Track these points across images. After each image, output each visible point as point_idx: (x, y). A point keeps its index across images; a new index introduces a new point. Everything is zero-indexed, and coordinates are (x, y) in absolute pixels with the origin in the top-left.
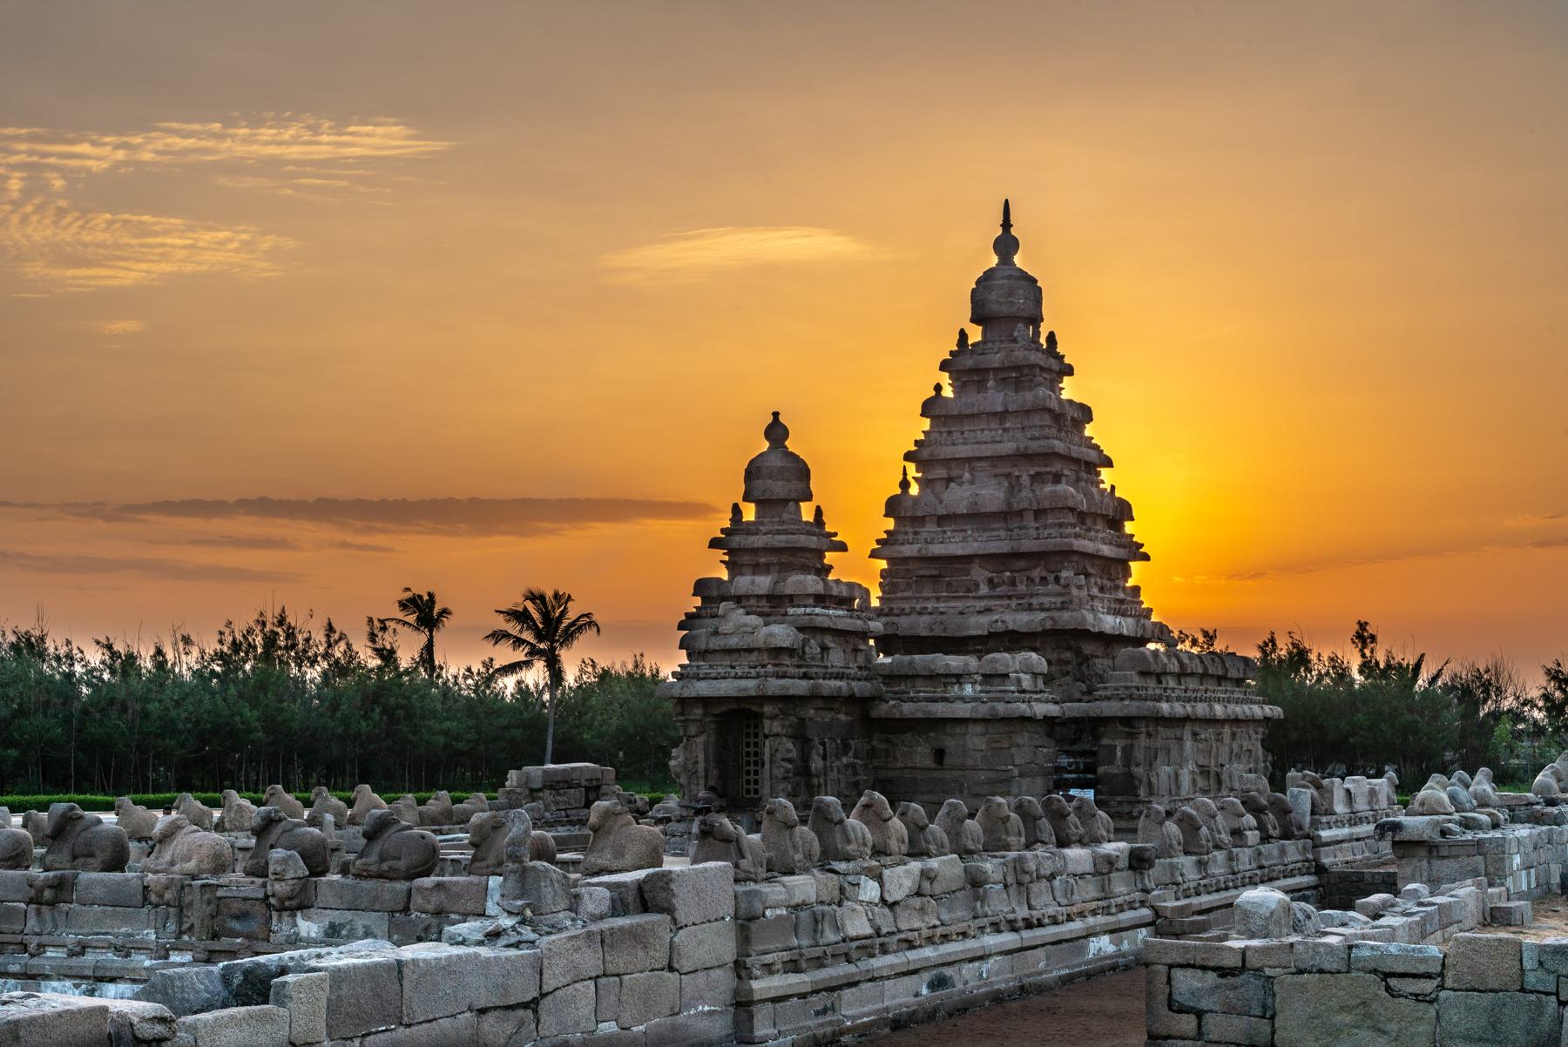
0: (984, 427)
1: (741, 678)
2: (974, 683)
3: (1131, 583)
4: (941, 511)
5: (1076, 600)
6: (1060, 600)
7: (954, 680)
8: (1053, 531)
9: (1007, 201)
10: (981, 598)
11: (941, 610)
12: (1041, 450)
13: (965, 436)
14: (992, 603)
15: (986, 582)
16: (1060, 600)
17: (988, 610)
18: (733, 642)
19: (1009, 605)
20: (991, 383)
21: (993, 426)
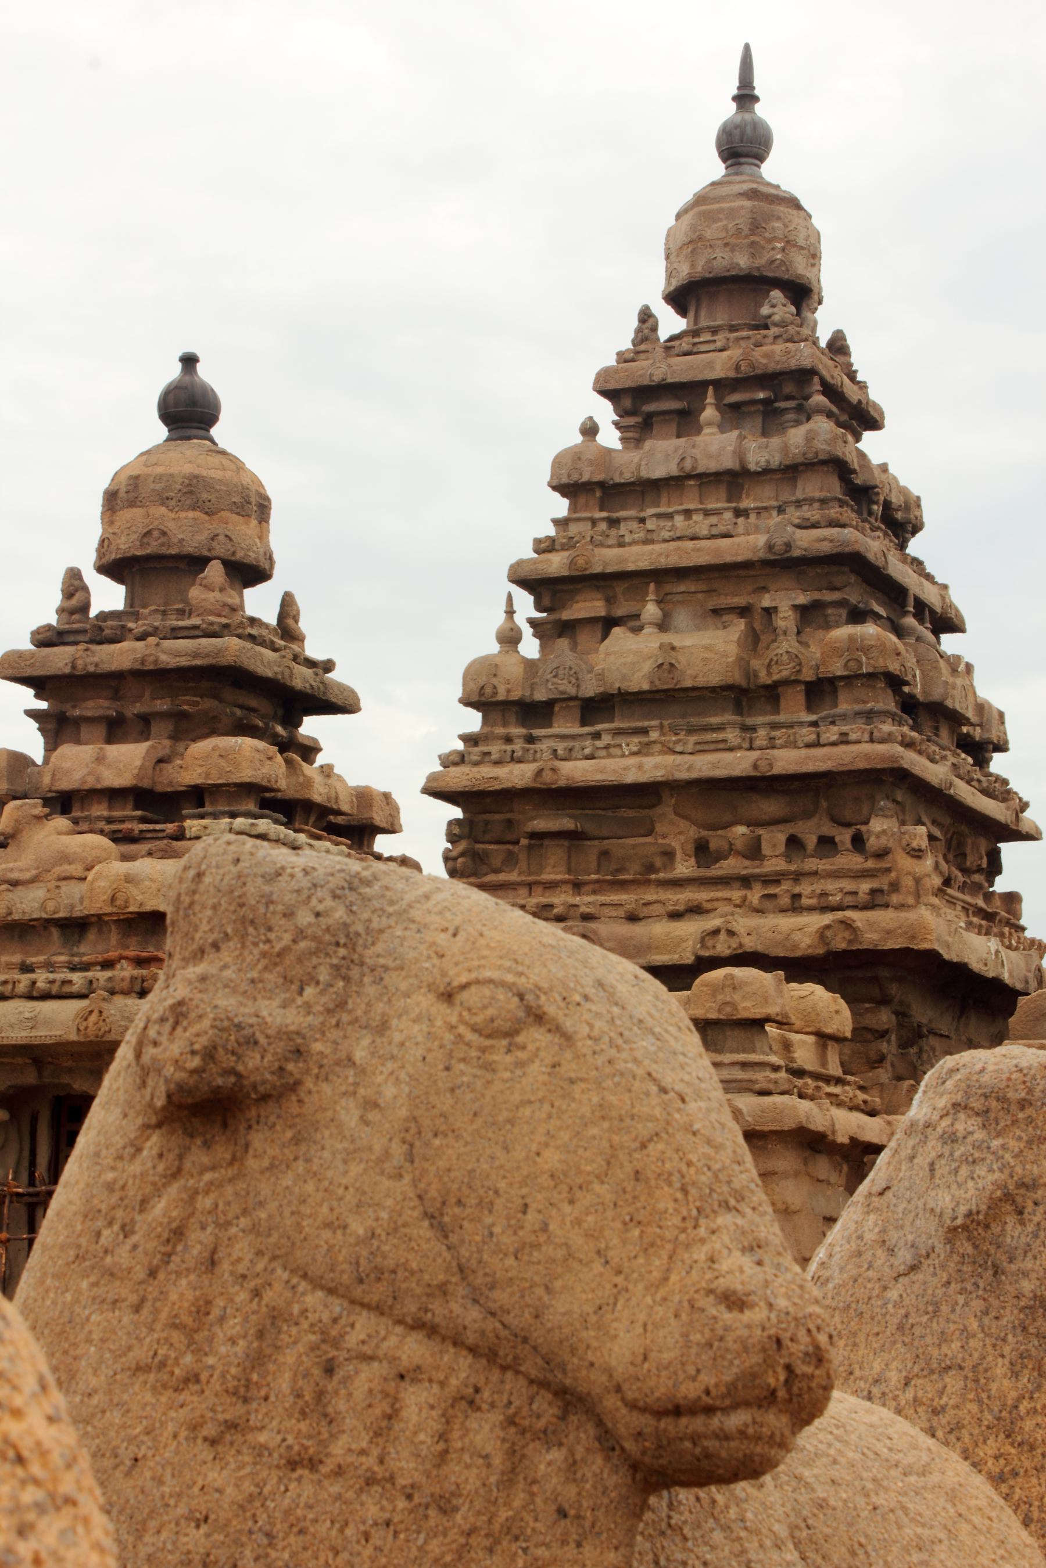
0: (691, 506)
1: (46, 996)
3: (1001, 885)
4: (590, 689)
5: (908, 882)
6: (865, 886)
9: (747, 48)
11: (584, 909)
12: (826, 548)
13: (650, 524)
14: (701, 895)
15: (690, 848)
16: (865, 886)
17: (696, 910)
19: (745, 899)
20: (709, 413)
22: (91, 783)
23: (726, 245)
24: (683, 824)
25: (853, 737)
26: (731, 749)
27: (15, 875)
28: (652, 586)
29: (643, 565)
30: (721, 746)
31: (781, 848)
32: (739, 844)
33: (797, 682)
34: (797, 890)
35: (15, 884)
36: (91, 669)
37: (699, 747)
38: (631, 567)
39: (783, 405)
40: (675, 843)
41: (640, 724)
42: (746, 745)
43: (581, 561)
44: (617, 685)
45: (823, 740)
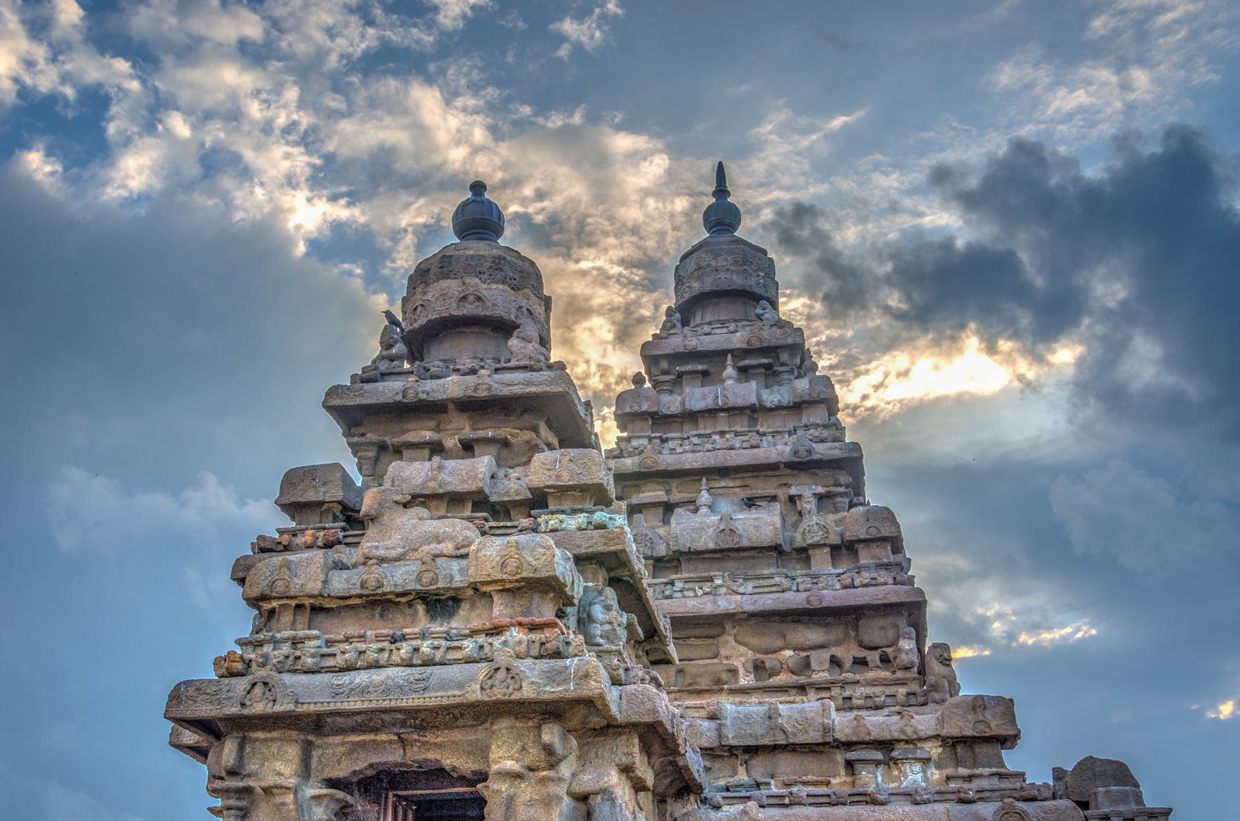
0: (726, 429)
2: (926, 761)
4: (662, 551)
6: (902, 690)
7: (879, 756)
8: (884, 576)
9: (720, 165)
10: (744, 691)
15: (750, 666)
18: (400, 577)
21: (738, 428)
22: (433, 487)
23: (728, 270)
24: (742, 649)
25: (881, 580)
26: (783, 592)
27: (381, 553)
28: (704, 479)
29: (696, 465)
30: (774, 589)
31: (828, 665)
32: (791, 663)
33: (824, 545)
34: (847, 693)
35: (382, 560)
36: (424, 396)
37: (756, 590)
38: (688, 466)
39: (780, 369)
40: (738, 663)
41: (706, 574)
42: (794, 588)
43: (649, 461)
44: (688, 545)
45: (857, 583)
